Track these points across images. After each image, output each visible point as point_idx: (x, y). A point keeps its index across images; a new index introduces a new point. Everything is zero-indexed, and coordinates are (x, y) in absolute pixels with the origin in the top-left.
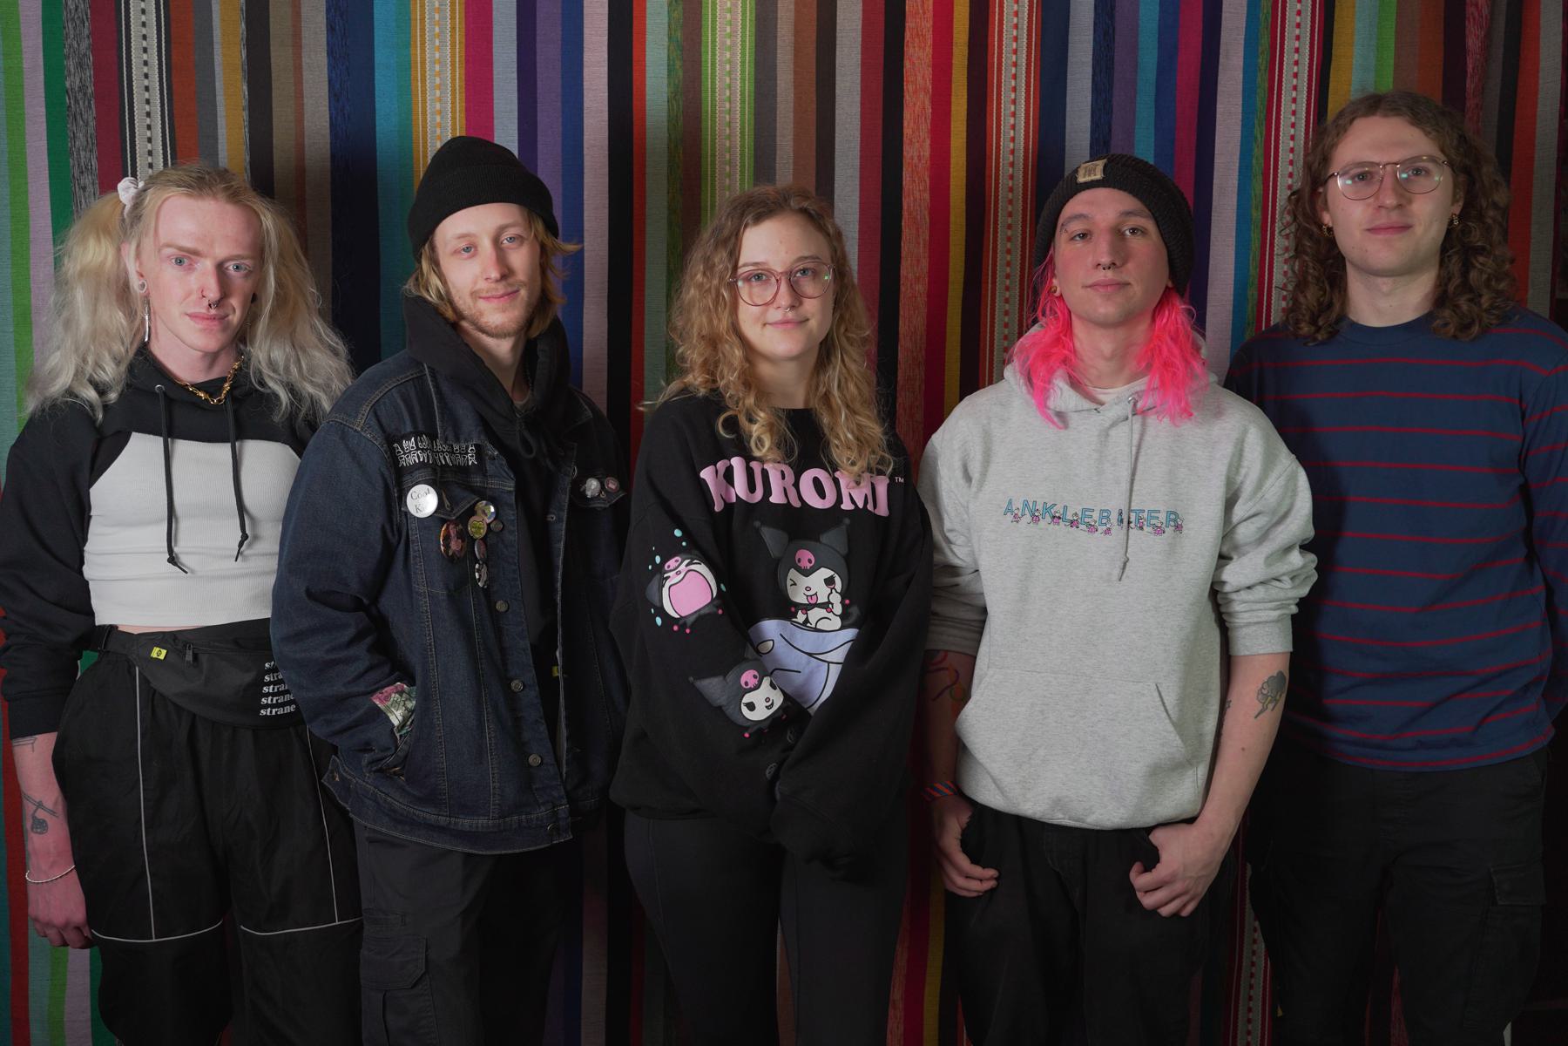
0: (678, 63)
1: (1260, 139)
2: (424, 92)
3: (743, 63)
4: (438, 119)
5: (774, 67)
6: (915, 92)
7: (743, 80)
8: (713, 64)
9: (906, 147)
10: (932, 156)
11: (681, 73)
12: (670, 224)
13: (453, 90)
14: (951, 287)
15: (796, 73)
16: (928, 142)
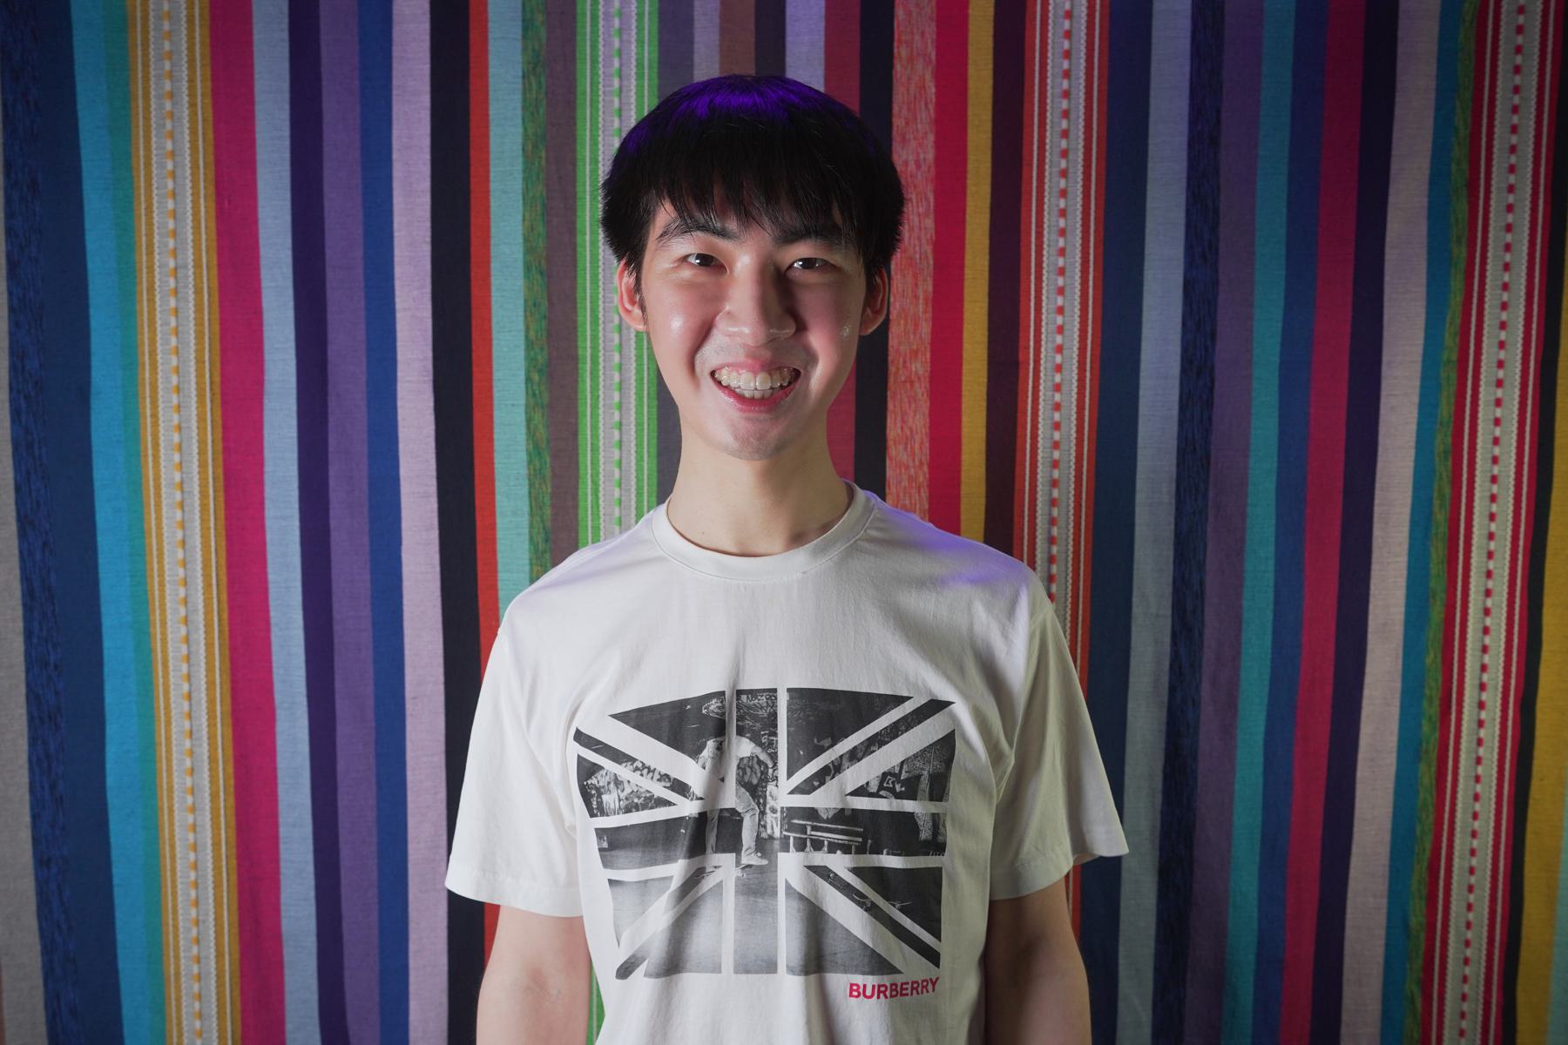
0: (540, 18)
1: (1464, 132)
2: (146, 65)
3: (640, 16)
4: (168, 106)
5: (689, 22)
6: (911, 59)
7: (640, 41)
8: (594, 18)
9: (896, 146)
10: (937, 159)
11: (543, 32)
12: (528, 268)
13: (191, 61)
14: (966, 368)
15: (724, 32)
16: (931, 138)
